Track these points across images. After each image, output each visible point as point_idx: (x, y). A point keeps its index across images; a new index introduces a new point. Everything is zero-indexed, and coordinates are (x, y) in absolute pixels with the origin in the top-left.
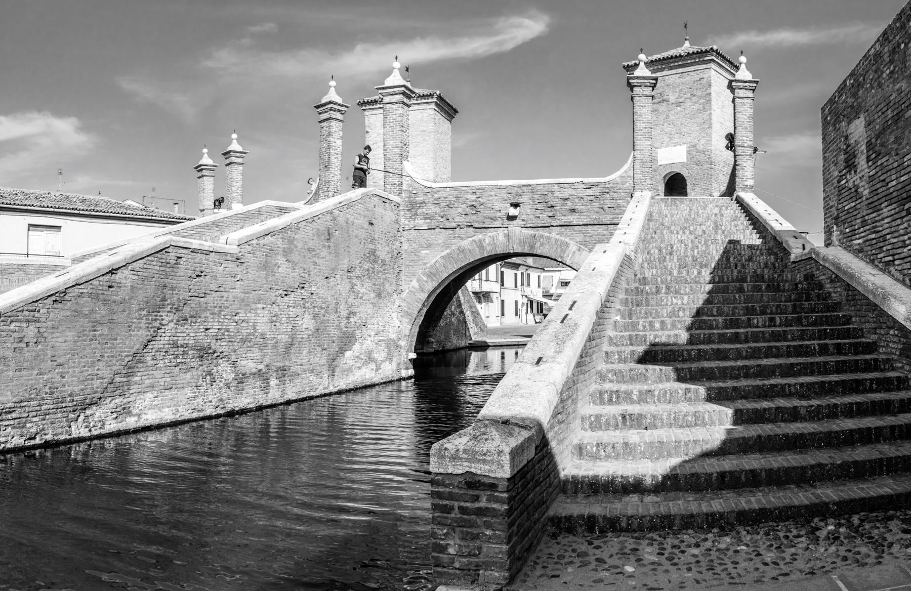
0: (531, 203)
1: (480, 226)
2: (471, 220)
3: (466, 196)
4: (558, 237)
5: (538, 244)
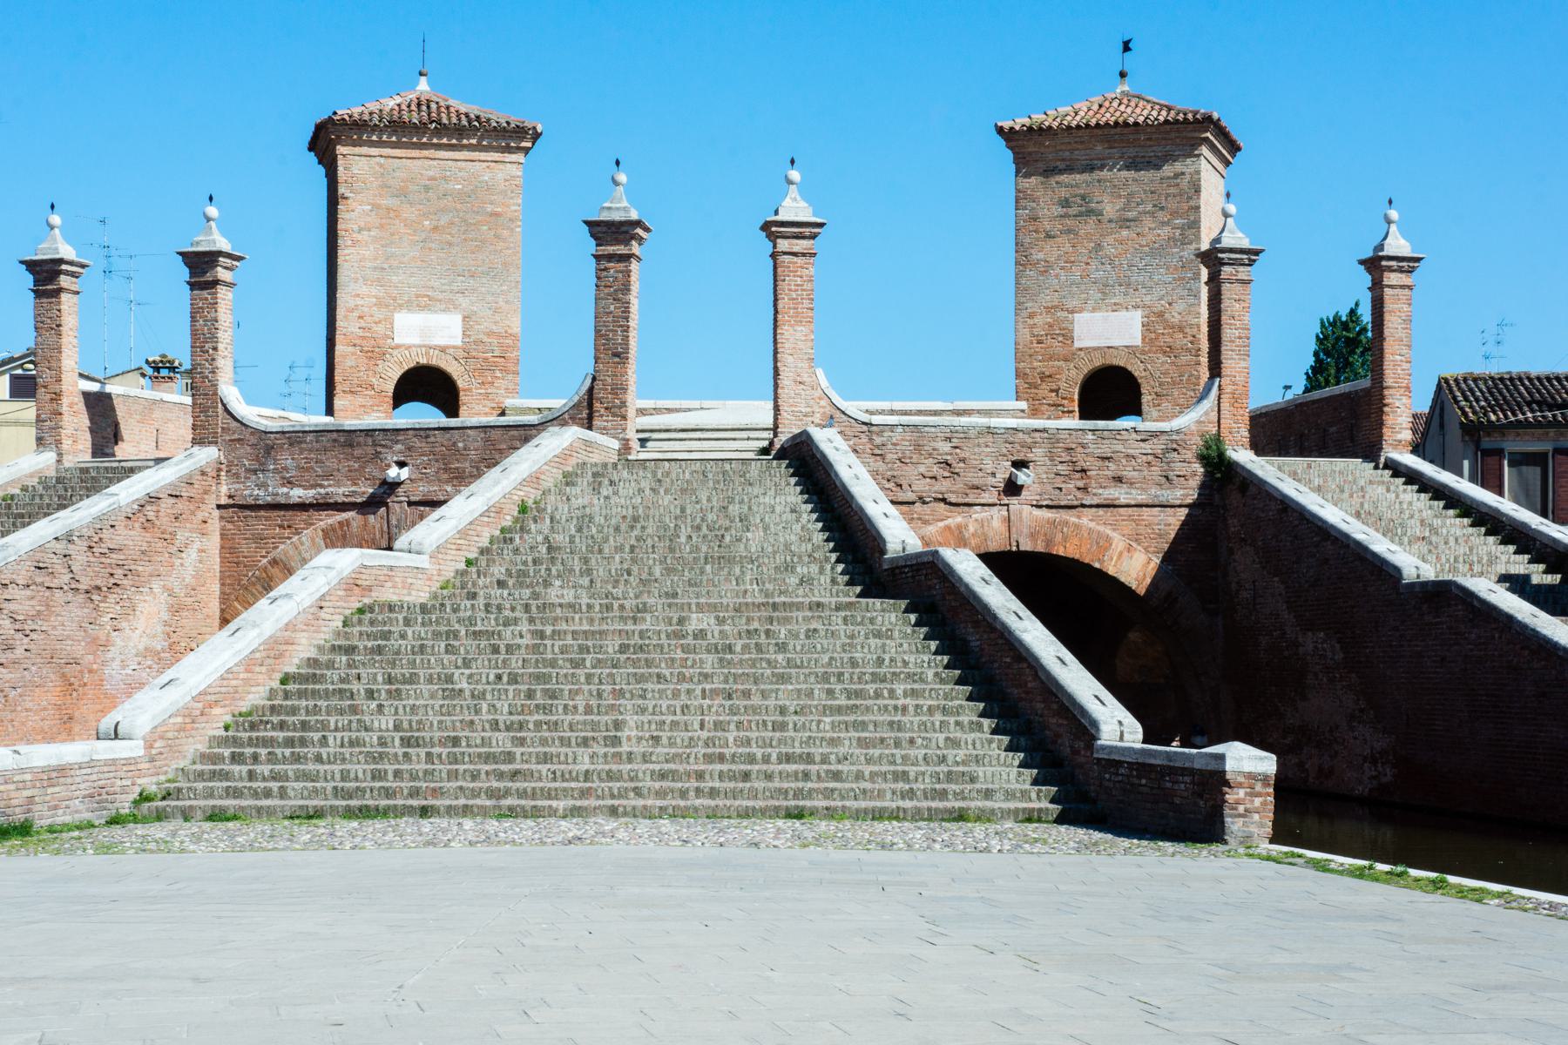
0: (1049, 463)
1: (960, 500)
2: (944, 489)
3: (933, 444)
4: (1092, 525)
5: (1059, 537)
